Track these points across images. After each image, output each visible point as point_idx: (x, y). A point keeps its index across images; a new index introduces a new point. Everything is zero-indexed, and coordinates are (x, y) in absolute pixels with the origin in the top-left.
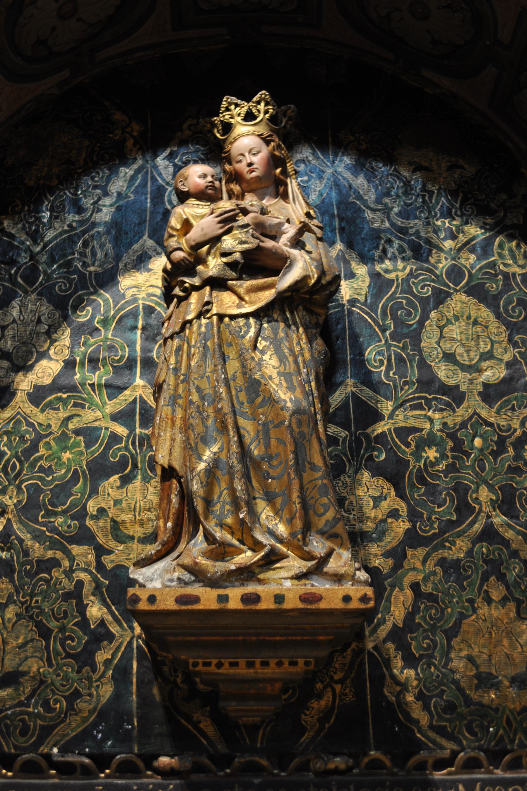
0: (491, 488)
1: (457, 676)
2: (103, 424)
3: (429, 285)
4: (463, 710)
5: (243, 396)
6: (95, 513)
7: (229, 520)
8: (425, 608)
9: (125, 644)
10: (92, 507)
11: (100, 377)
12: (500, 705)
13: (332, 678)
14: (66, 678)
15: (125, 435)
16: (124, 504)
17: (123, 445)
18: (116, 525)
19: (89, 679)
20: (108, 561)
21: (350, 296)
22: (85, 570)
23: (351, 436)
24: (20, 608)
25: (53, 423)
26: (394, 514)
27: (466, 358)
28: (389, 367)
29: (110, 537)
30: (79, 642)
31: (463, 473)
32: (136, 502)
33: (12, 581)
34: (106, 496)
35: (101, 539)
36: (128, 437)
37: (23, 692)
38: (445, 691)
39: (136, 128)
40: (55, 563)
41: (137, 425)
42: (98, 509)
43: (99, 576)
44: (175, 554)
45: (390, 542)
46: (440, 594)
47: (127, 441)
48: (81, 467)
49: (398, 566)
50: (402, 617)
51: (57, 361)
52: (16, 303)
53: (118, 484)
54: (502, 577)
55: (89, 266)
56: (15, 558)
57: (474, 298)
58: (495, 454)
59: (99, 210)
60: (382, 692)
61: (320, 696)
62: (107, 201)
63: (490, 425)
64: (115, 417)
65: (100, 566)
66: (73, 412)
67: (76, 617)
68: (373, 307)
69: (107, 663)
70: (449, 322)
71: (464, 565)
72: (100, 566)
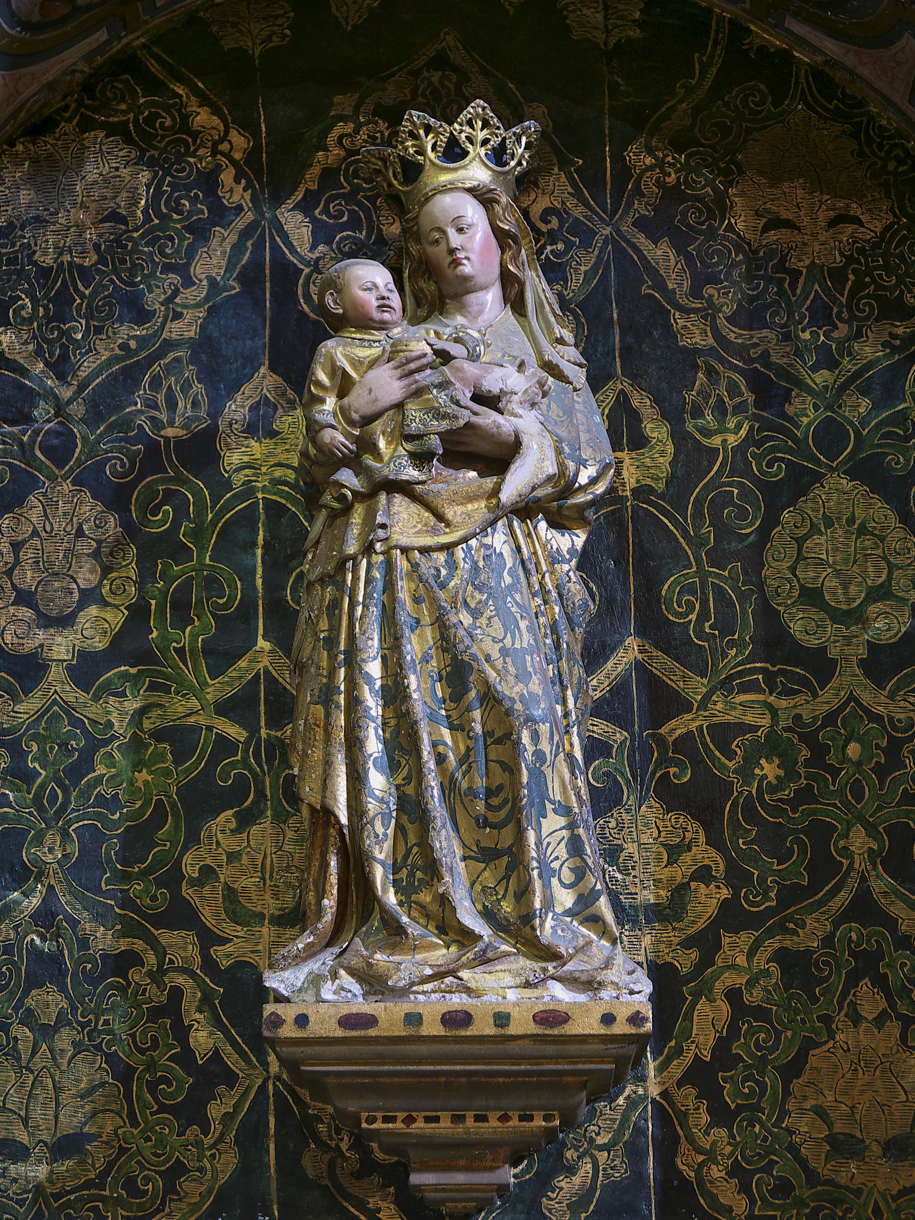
0: (871, 830)
2: (202, 720)
3: (782, 460)
4: (806, 1193)
6: (196, 875)
8: (747, 1031)
9: (255, 1088)
10: (190, 866)
11: (194, 637)
12: (865, 1185)
13: (592, 1140)
14: (161, 1142)
15: (242, 740)
16: (245, 860)
17: (239, 757)
18: (230, 894)
19: (198, 1144)
20: (223, 955)
21: (638, 481)
23: (633, 740)
24: (79, 1033)
25: (114, 718)
26: (703, 874)
27: (842, 598)
28: (703, 616)
29: (223, 916)
30: (180, 1088)
31: (824, 804)
32: (265, 857)
33: (63, 989)
34: (214, 847)
36: (247, 743)
37: (93, 1166)
38: (777, 1162)
41: (263, 723)
42: (201, 868)
43: (207, 980)
45: (694, 922)
46: (775, 1008)
47: (246, 751)
48: (170, 797)
49: (707, 960)
50: (711, 1043)
51: (117, 607)
53: (234, 825)
54: (880, 981)
55: (164, 428)
56: (66, 952)
57: (864, 483)
58: (882, 771)
59: (178, 316)
60: (673, 1163)
61: (571, 1171)
62: (190, 295)
63: (878, 718)
64: (224, 708)
65: (209, 964)
66: (151, 700)
67: (172, 1047)
69: (228, 1118)
70: (814, 529)
71: (817, 961)
72: (209, 964)
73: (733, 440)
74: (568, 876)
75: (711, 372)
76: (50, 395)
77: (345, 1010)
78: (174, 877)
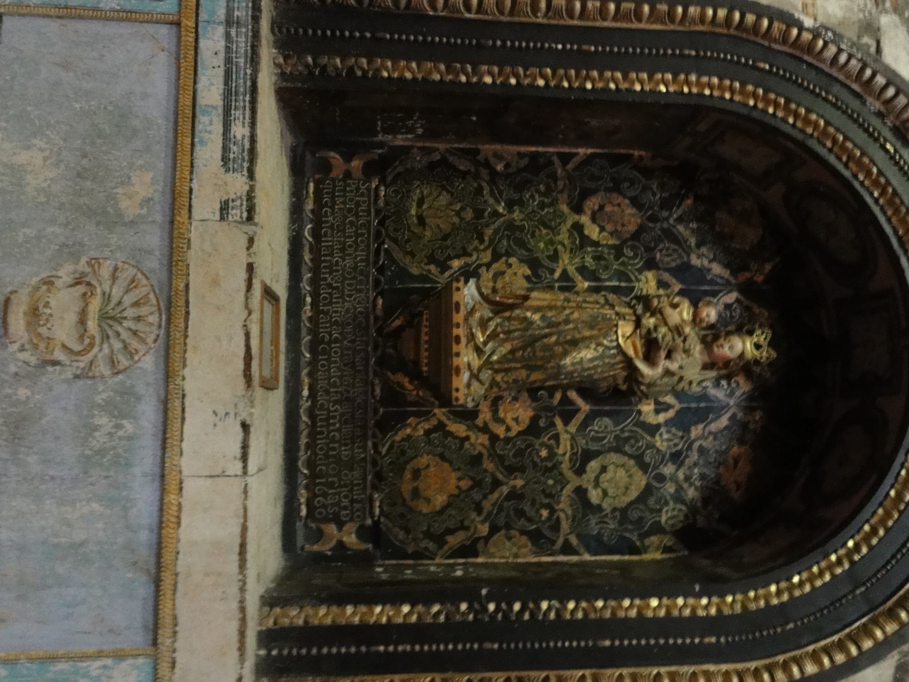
0: (523, 487)
1: (419, 458)
5: (569, 337)
7: (499, 329)
10: (513, 260)
14: (422, 250)
18: (503, 273)
19: (421, 262)
20: (483, 270)
22: (478, 257)
26: (508, 429)
28: (597, 432)
33: (472, 219)
35: (495, 266)
39: (759, 278)
40: (482, 241)
44: (482, 301)
52: (634, 211)
53: (526, 274)
54: (471, 488)
58: (543, 491)
59: (698, 258)
60: (411, 416)
61: (410, 382)
62: (706, 262)
63: (562, 490)
64: (565, 272)
65: (480, 266)
68: (635, 425)
69: (429, 271)
70: (627, 471)
72: (480, 266)
73: (658, 444)
74: (506, 379)
75: (682, 438)
76: (670, 216)
77: (462, 303)
78: (508, 254)
